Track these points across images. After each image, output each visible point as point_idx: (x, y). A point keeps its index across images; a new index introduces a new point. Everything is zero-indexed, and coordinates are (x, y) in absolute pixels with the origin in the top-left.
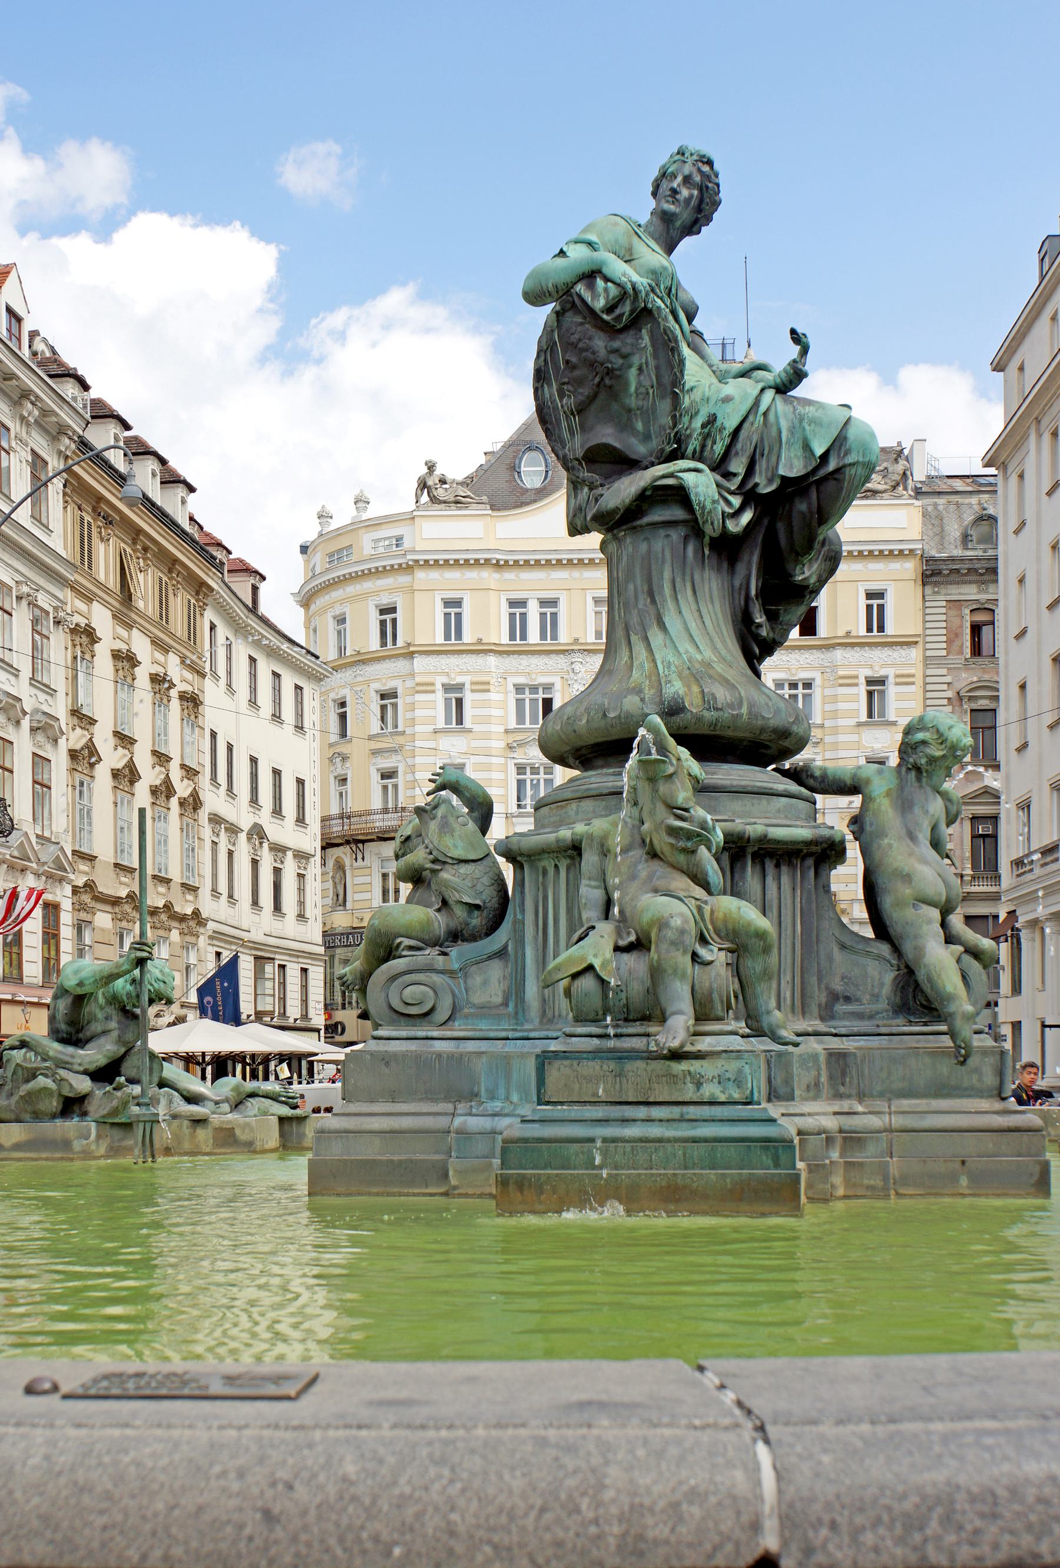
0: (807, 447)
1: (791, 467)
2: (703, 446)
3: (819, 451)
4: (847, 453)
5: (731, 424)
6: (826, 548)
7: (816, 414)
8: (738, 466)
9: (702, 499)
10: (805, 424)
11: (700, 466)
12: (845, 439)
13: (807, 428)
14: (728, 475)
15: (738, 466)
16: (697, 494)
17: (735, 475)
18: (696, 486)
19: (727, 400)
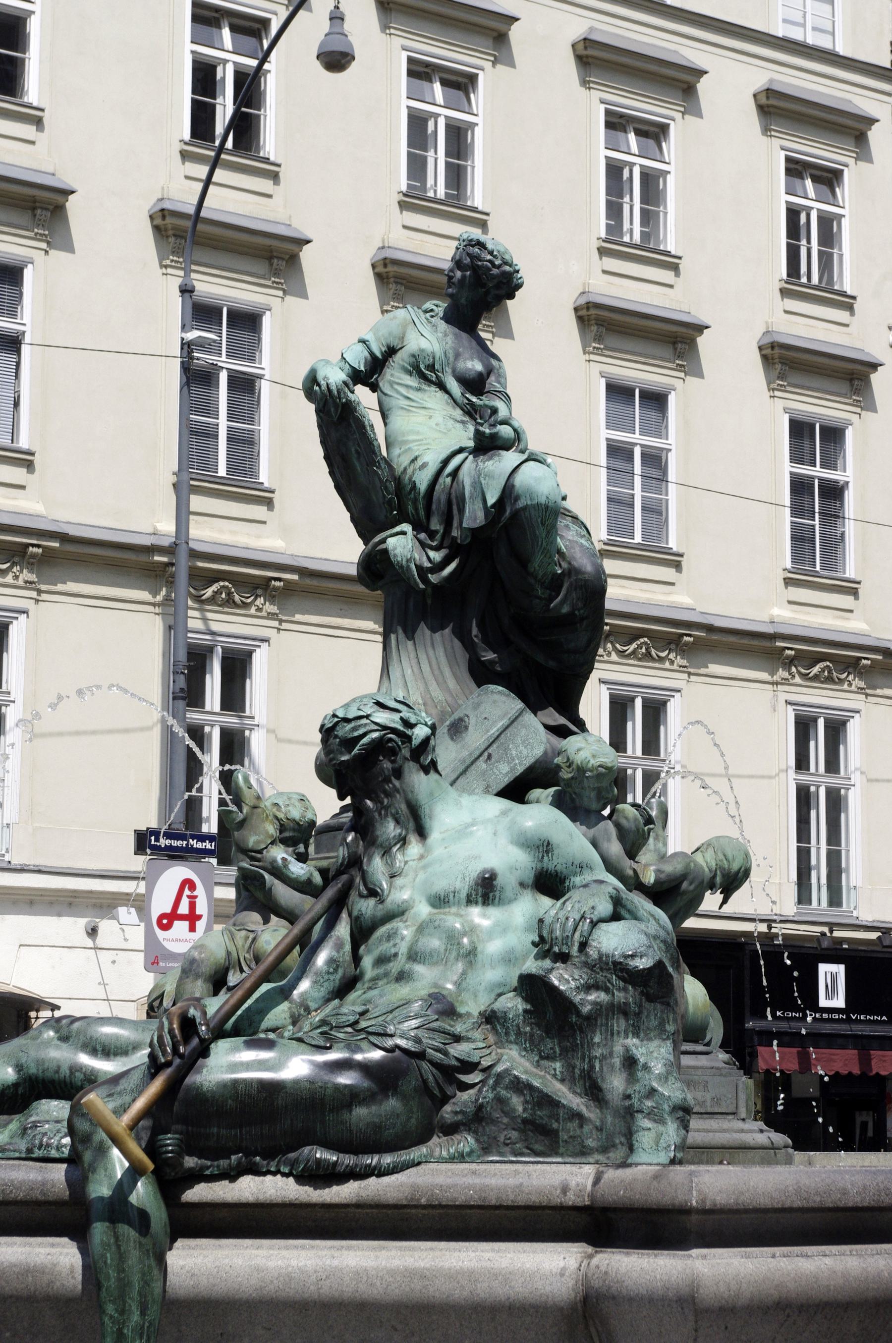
0: (484, 501)
1: (476, 519)
2: (416, 509)
3: (491, 501)
4: (517, 498)
5: (422, 486)
6: (573, 578)
7: (491, 468)
8: (436, 525)
9: (399, 559)
10: (482, 479)
11: (406, 527)
12: (513, 486)
13: (483, 482)
14: (432, 535)
15: (436, 525)
16: (395, 556)
17: (437, 532)
18: (395, 549)
19: (424, 466)
